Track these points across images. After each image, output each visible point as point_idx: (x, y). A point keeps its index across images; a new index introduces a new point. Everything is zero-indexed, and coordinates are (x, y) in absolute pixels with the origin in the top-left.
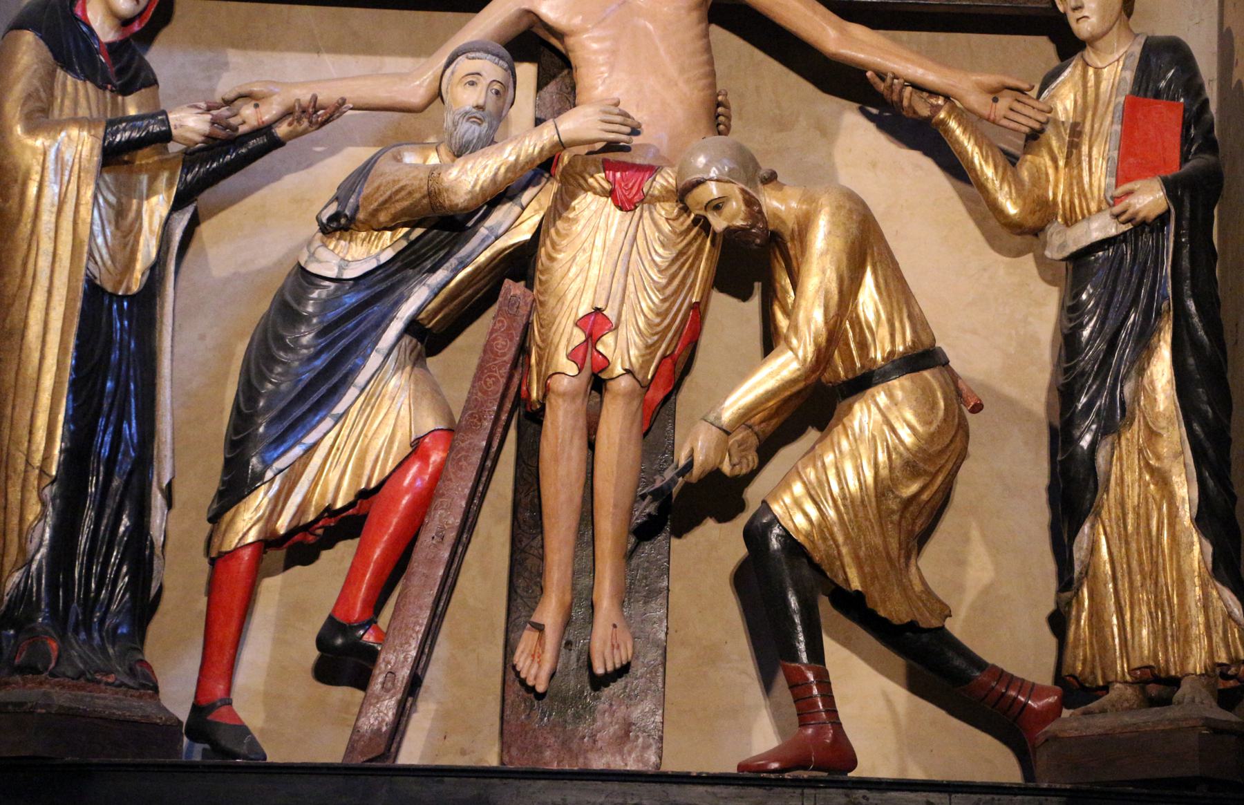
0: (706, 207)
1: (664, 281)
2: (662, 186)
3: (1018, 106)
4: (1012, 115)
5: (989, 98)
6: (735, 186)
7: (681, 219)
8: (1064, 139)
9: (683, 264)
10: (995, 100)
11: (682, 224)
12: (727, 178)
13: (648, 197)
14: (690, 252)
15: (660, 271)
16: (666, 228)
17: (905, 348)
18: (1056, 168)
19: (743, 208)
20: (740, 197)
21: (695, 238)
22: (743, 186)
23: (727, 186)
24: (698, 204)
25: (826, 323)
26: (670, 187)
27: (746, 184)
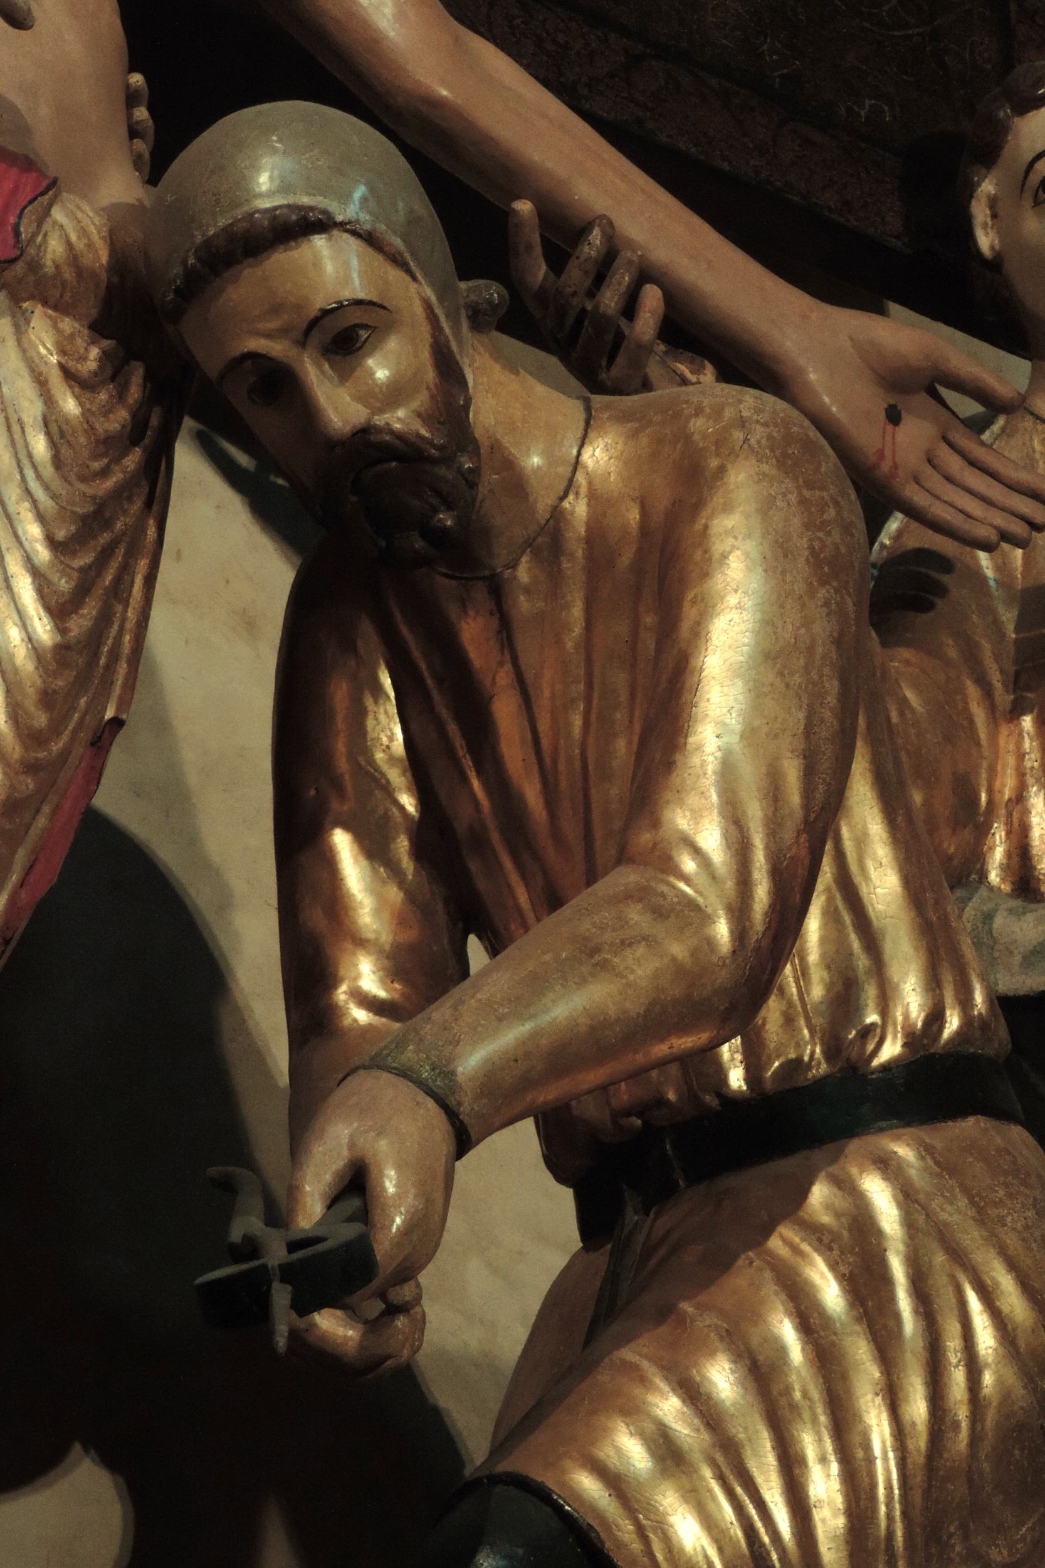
0: (314, 323)
1: (64, 585)
2: (69, 245)
3: (954, 464)
4: (936, 482)
5: (875, 402)
6: (413, 286)
7: (103, 396)
8: (1002, 635)
9: (106, 554)
10: (894, 416)
11: (107, 411)
12: (398, 242)
13: (19, 268)
14: (119, 525)
15: (51, 541)
16: (70, 406)
17: (967, 1021)
18: (992, 708)
19: (430, 375)
20: (425, 329)
21: (120, 494)
22: (433, 299)
23: (394, 274)
24: (276, 309)
25: (807, 805)
26: (87, 260)
27: (441, 299)
